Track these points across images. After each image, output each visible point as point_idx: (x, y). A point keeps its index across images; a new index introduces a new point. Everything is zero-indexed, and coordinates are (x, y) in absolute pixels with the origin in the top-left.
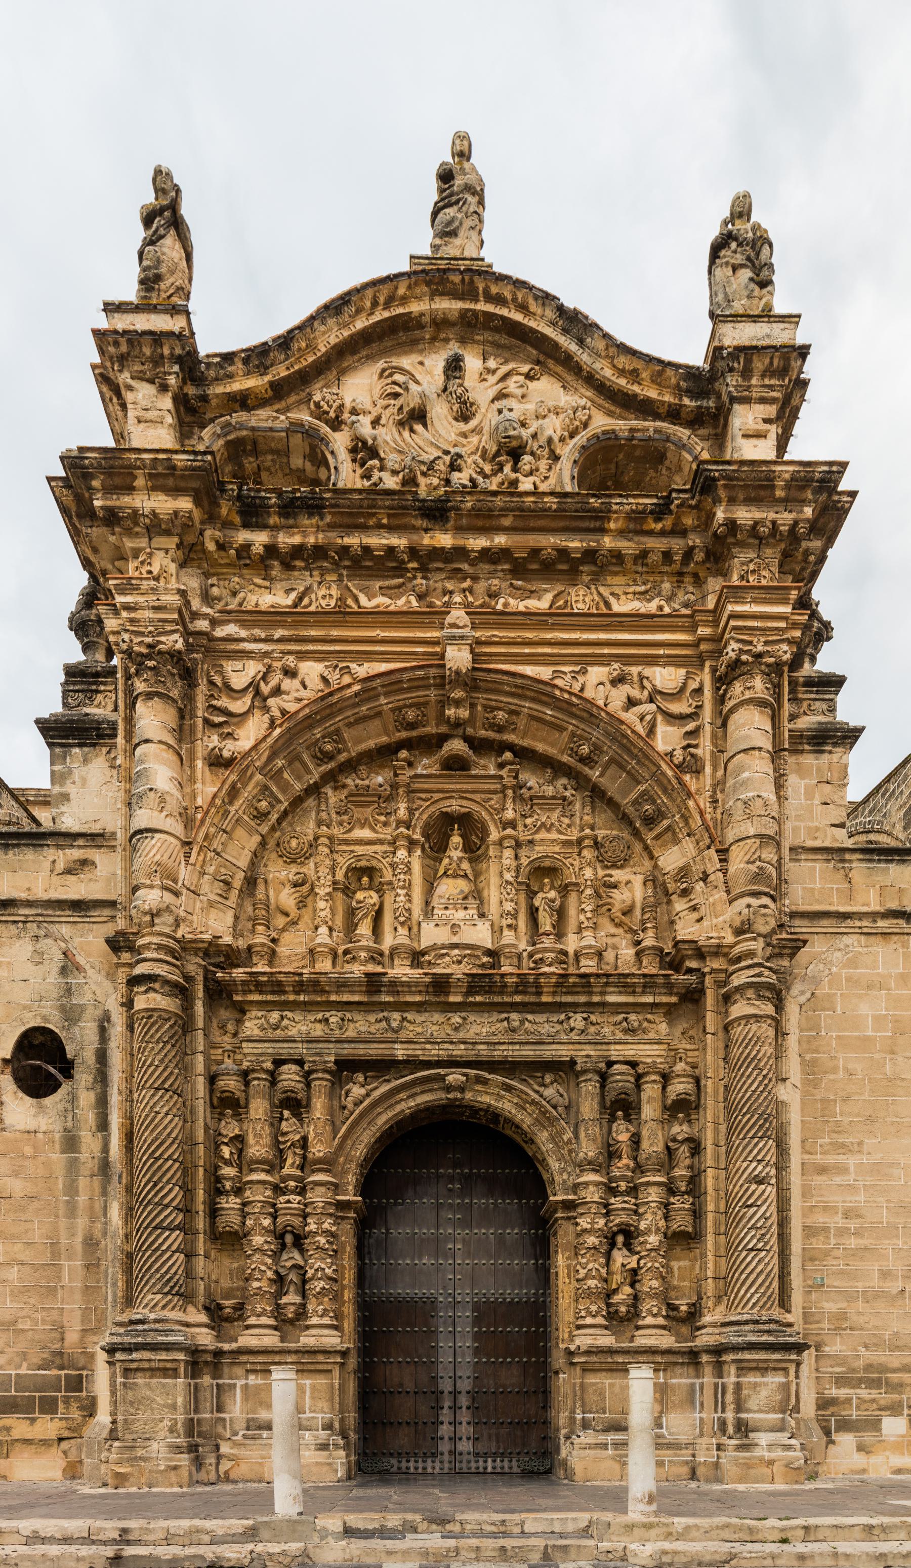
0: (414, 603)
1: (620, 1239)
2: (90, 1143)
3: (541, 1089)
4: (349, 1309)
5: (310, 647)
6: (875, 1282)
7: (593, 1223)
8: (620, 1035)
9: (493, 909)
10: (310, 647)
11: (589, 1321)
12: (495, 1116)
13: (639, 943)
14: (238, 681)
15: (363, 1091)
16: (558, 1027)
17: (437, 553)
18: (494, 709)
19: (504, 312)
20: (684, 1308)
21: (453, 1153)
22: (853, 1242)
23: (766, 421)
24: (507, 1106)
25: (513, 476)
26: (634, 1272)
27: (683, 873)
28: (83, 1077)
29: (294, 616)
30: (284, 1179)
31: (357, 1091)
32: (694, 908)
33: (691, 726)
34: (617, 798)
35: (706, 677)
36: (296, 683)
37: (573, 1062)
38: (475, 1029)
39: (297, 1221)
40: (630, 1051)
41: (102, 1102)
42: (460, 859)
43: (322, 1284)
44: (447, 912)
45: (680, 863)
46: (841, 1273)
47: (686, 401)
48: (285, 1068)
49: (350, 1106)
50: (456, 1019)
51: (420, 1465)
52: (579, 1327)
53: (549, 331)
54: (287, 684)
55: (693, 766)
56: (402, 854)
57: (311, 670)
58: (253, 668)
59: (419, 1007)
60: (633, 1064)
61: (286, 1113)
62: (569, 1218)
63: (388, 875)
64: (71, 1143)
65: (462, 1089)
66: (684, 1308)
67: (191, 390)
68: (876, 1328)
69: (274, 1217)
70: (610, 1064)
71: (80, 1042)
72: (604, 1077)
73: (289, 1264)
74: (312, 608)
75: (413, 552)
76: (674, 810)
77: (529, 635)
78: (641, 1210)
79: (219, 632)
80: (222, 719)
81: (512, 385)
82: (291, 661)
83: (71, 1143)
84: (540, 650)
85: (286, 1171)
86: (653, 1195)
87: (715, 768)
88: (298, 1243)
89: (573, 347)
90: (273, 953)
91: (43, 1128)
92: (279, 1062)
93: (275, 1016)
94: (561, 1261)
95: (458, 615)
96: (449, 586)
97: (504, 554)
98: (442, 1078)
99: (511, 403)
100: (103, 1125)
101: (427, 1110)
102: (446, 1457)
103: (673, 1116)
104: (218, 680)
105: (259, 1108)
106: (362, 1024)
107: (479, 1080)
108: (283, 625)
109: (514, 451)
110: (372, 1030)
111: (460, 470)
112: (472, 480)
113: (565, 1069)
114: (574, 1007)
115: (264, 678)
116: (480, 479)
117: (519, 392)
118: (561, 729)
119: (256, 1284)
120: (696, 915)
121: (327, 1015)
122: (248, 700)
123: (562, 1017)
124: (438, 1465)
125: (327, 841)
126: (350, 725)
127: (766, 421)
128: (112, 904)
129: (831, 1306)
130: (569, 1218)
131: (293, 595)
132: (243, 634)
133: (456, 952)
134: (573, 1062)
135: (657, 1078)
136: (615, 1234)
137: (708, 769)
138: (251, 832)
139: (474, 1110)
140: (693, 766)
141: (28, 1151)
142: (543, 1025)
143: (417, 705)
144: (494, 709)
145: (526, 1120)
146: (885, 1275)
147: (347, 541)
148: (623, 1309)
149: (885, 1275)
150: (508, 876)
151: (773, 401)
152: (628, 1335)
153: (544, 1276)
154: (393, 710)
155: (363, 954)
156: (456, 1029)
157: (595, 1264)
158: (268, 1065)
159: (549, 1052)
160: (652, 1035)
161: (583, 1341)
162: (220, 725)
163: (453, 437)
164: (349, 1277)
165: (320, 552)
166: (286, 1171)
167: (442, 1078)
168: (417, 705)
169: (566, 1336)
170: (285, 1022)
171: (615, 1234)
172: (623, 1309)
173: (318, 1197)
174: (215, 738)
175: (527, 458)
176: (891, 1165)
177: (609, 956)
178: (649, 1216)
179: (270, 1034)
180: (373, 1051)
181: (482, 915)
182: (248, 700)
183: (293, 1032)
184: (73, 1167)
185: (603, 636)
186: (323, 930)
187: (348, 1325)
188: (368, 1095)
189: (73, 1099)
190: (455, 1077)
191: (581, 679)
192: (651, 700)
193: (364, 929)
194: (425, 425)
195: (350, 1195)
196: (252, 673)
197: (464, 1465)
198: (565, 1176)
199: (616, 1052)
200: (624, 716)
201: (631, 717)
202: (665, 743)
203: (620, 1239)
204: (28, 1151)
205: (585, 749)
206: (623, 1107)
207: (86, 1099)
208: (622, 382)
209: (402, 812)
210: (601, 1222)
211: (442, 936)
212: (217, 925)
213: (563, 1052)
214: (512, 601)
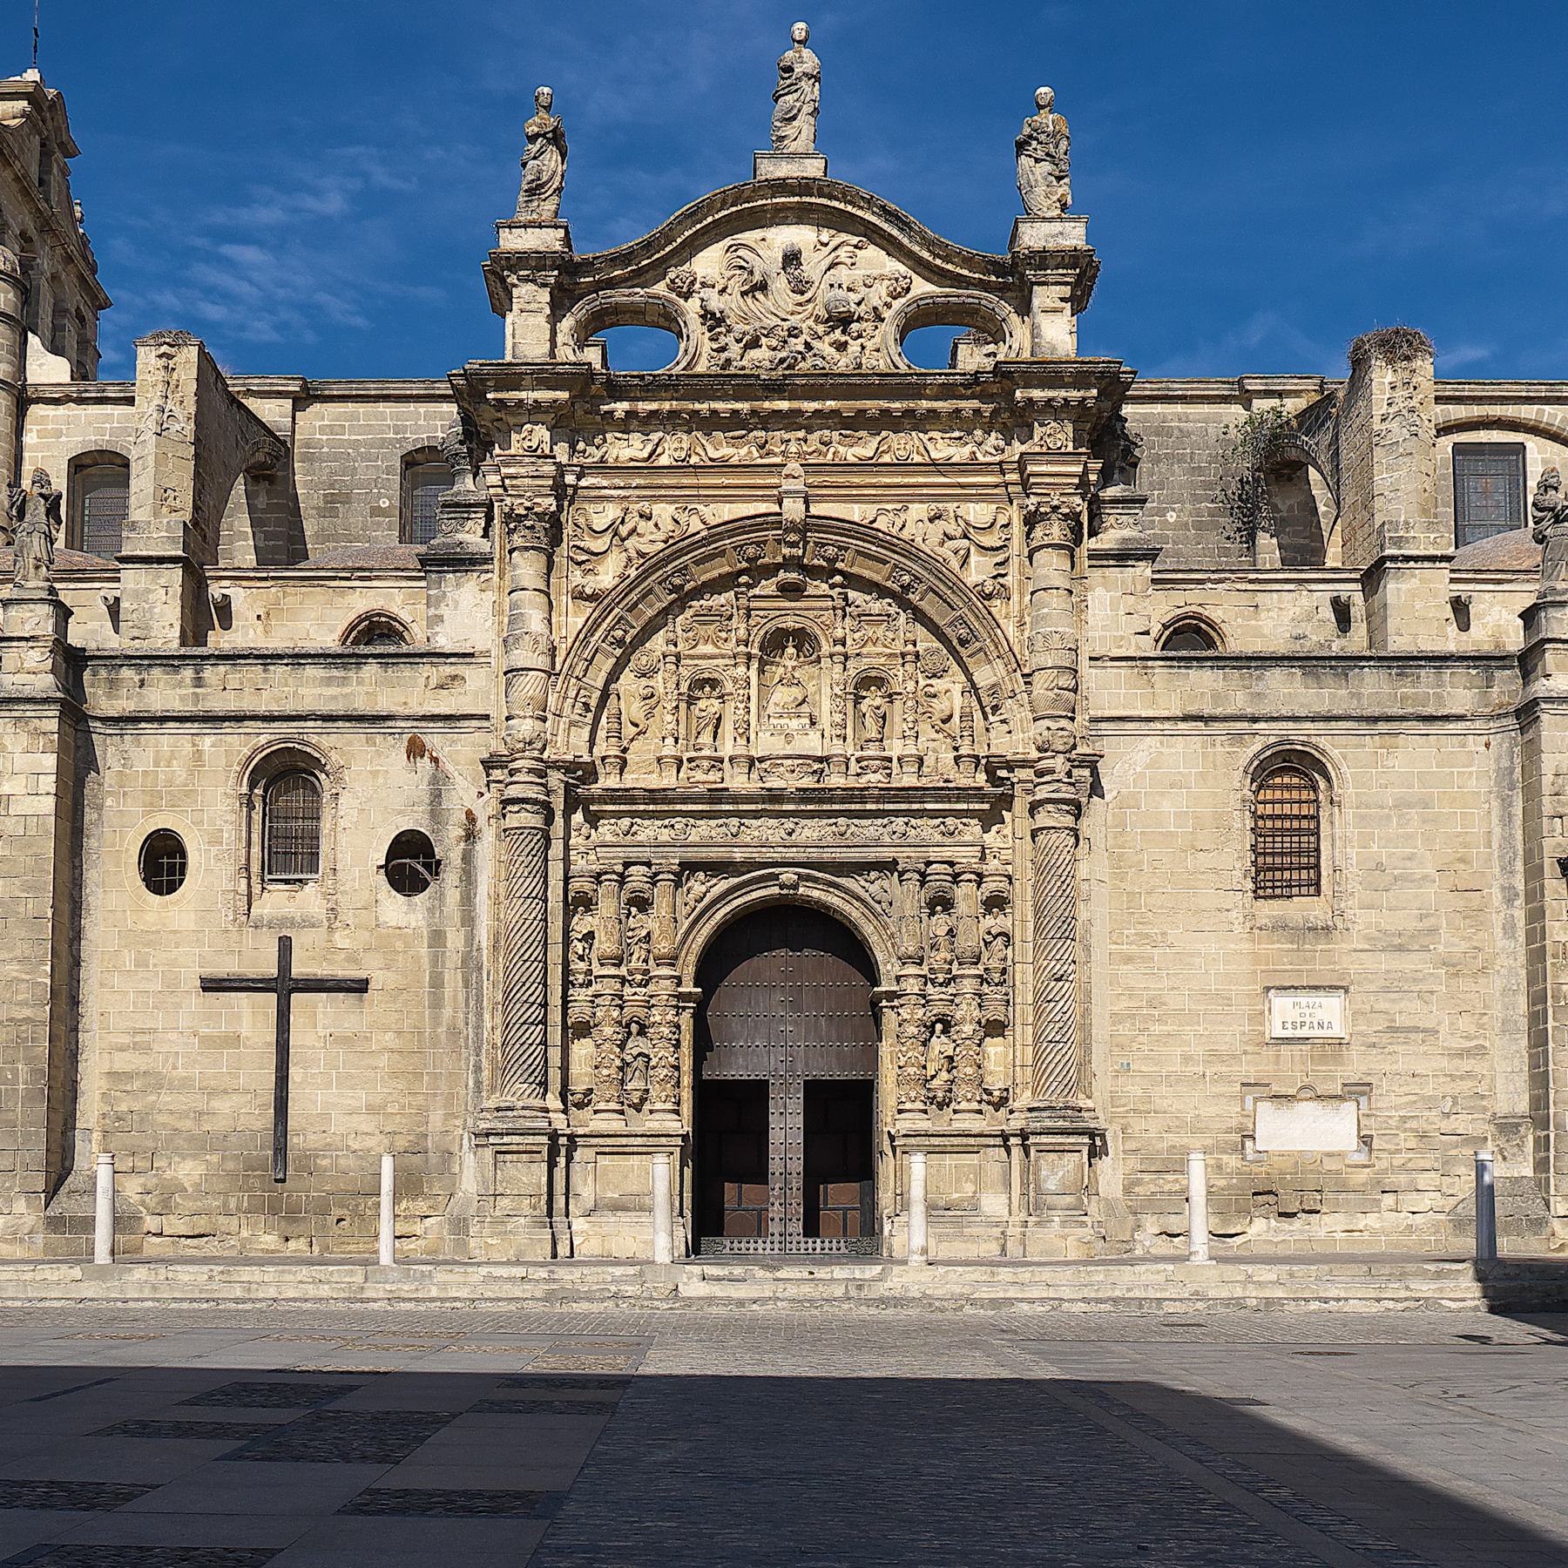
0: (756, 454)
1: (939, 1027)
2: (455, 939)
3: (867, 885)
4: (687, 1095)
5: (663, 492)
6: (1177, 1067)
7: (912, 1014)
8: (938, 838)
9: (825, 721)
10: (663, 492)
11: (908, 1106)
12: (828, 908)
13: (956, 749)
14: (600, 523)
15: (703, 889)
16: (881, 830)
17: (777, 413)
18: (824, 545)
19: (835, 204)
20: (996, 1093)
21: (782, 932)
22: (1157, 1028)
23: (1062, 299)
24: (834, 900)
25: (843, 339)
26: (951, 1059)
27: (994, 689)
28: (451, 876)
29: (647, 467)
30: (630, 973)
31: (698, 889)
32: (1003, 721)
33: (1000, 559)
34: (936, 619)
35: (1015, 514)
36: (651, 523)
37: (895, 862)
38: (807, 832)
39: (642, 1012)
40: (947, 853)
41: (468, 900)
42: (794, 668)
43: (665, 1071)
44: (782, 721)
45: (993, 680)
46: (1147, 1057)
47: (993, 278)
48: (633, 869)
49: (692, 903)
50: (789, 824)
51: (752, 1245)
52: (900, 1111)
53: (873, 219)
54: (643, 526)
55: (1004, 593)
56: (742, 669)
57: (664, 512)
58: (612, 512)
59: (756, 815)
60: (952, 864)
61: (634, 910)
62: (892, 1008)
63: (729, 687)
64: (437, 938)
65: (795, 887)
66: (996, 1093)
67: (566, 280)
68: (1179, 1111)
69: (622, 1008)
70: (929, 864)
71: (448, 847)
72: (923, 875)
73: (635, 1052)
74: (664, 461)
75: (754, 412)
76: (985, 635)
77: (856, 480)
78: (957, 1001)
79: (583, 483)
80: (584, 558)
81: (843, 253)
82: (645, 506)
83: (437, 938)
84: (866, 492)
85: (633, 965)
86: (968, 986)
87: (1022, 595)
88: (642, 1032)
89: (895, 232)
90: (625, 761)
91: (413, 925)
92: (627, 865)
93: (626, 822)
94: (886, 1048)
95: (794, 467)
96: (786, 436)
97: (835, 413)
98: (776, 877)
99: (842, 274)
100: (469, 920)
101: (763, 900)
102: (777, 1238)
103: (988, 911)
104: (581, 521)
105: (608, 905)
106: (703, 830)
107: (809, 878)
108: (640, 475)
109: (843, 321)
110: (713, 833)
111: (796, 337)
112: (807, 344)
113: (888, 867)
114: (897, 813)
115: (623, 522)
116: (815, 343)
117: (849, 261)
118: (885, 562)
119: (605, 1072)
120: (1005, 728)
121: (673, 821)
122: (607, 537)
123: (885, 821)
124: (768, 1245)
125: (673, 659)
126: (697, 563)
127: (1062, 299)
128: (487, 717)
129: (1135, 1090)
130: (892, 1008)
131: (649, 448)
132: (605, 483)
133: (790, 762)
134: (895, 862)
135: (973, 877)
136: (933, 1024)
137: (1015, 597)
138: (607, 655)
139: (807, 900)
140: (1004, 593)
141: (399, 945)
142: (869, 829)
143: (758, 544)
144: (824, 545)
145: (854, 912)
146: (1187, 1059)
147: (697, 406)
148: (940, 1094)
149: (1187, 1059)
150: (837, 690)
151: (1066, 284)
152: (947, 1118)
153: (872, 1058)
154: (735, 548)
155: (706, 764)
156: (790, 834)
157: (915, 1053)
158: (619, 868)
159: (872, 854)
160: (967, 838)
161: (904, 1125)
162: (583, 562)
163: (791, 308)
164: (687, 1065)
165: (673, 414)
166: (633, 965)
167: (776, 877)
168: (758, 544)
169: (889, 1120)
170: (635, 828)
171: (933, 1024)
172: (940, 1094)
173: (663, 989)
174: (578, 573)
175: (854, 326)
176: (1192, 955)
177: (929, 761)
178: (964, 1006)
179: (621, 839)
180: (714, 854)
181: (813, 724)
182: (607, 537)
183: (640, 838)
184: (436, 960)
185: (921, 480)
186: (670, 741)
187: (687, 1109)
188: (708, 891)
189: (441, 897)
190: (788, 876)
191: (903, 516)
192: (966, 537)
193: (706, 738)
194: (766, 296)
195: (688, 987)
196: (611, 517)
197: (794, 1246)
198: (889, 967)
199: (933, 853)
200: (939, 550)
201: (945, 551)
202: (978, 572)
203: (939, 1027)
204: (399, 945)
205: (907, 579)
206: (941, 903)
207: (453, 896)
208: (938, 262)
209: (742, 633)
210: (921, 1012)
211: (776, 746)
212: (571, 743)
213: (887, 854)
214: (841, 449)
